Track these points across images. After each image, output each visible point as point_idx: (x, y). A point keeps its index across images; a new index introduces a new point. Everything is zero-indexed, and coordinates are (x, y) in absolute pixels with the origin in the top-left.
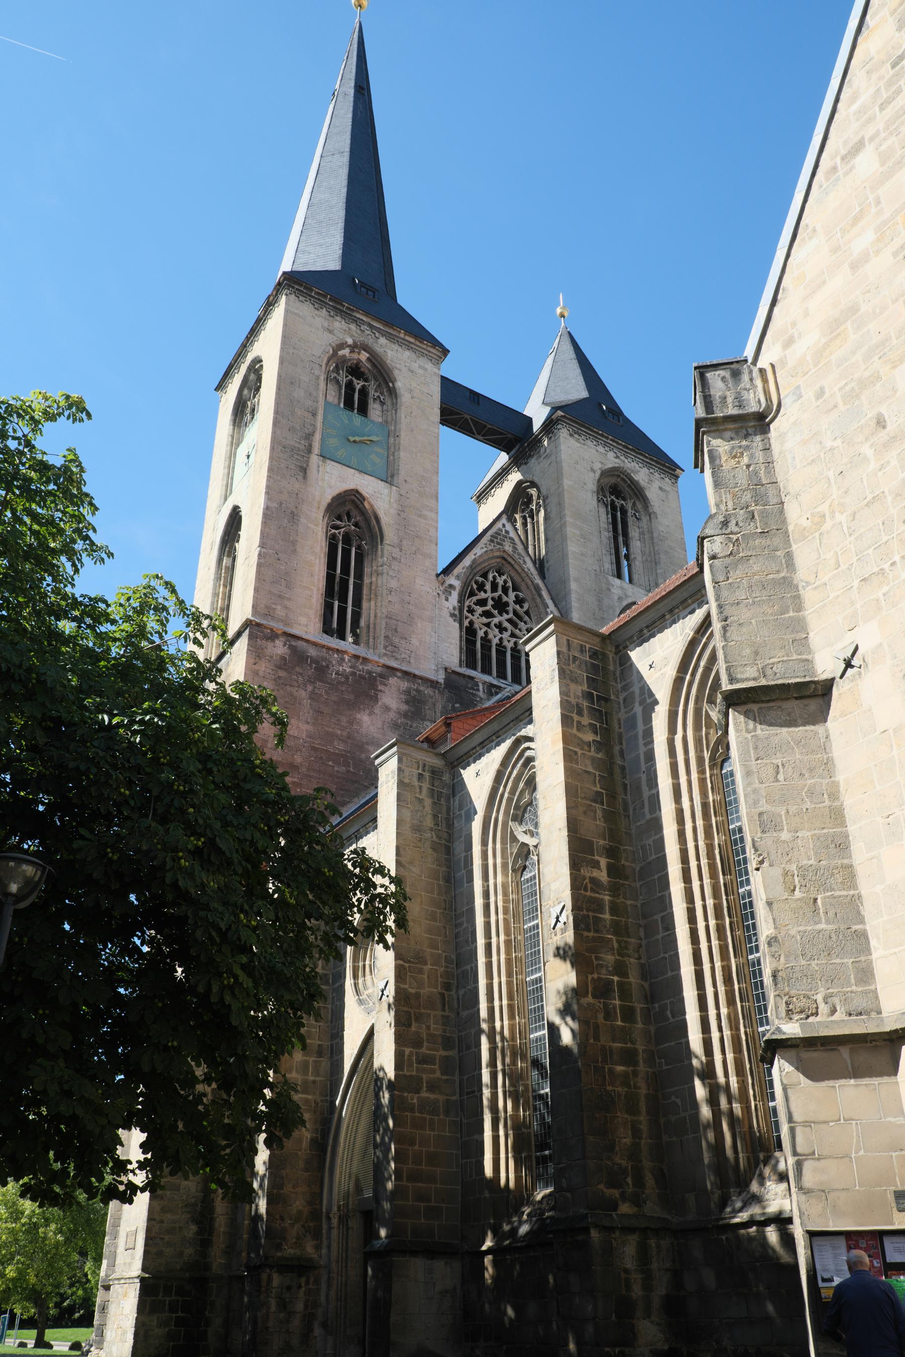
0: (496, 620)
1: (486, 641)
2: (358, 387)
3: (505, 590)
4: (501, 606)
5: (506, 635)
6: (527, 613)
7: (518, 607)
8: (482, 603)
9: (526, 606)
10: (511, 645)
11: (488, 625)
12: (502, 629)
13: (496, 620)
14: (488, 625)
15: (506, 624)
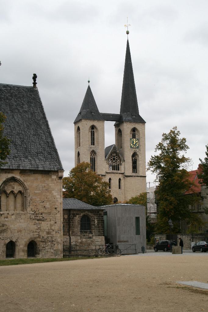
0: (113, 162)
1: (112, 165)
2: (93, 131)
3: (115, 157)
4: (114, 159)
5: (115, 163)
6: (118, 159)
7: (117, 159)
8: (112, 159)
9: (118, 158)
10: (115, 165)
11: (112, 163)
12: (114, 163)
13: (113, 162)
14: (112, 163)
15: (115, 162)
